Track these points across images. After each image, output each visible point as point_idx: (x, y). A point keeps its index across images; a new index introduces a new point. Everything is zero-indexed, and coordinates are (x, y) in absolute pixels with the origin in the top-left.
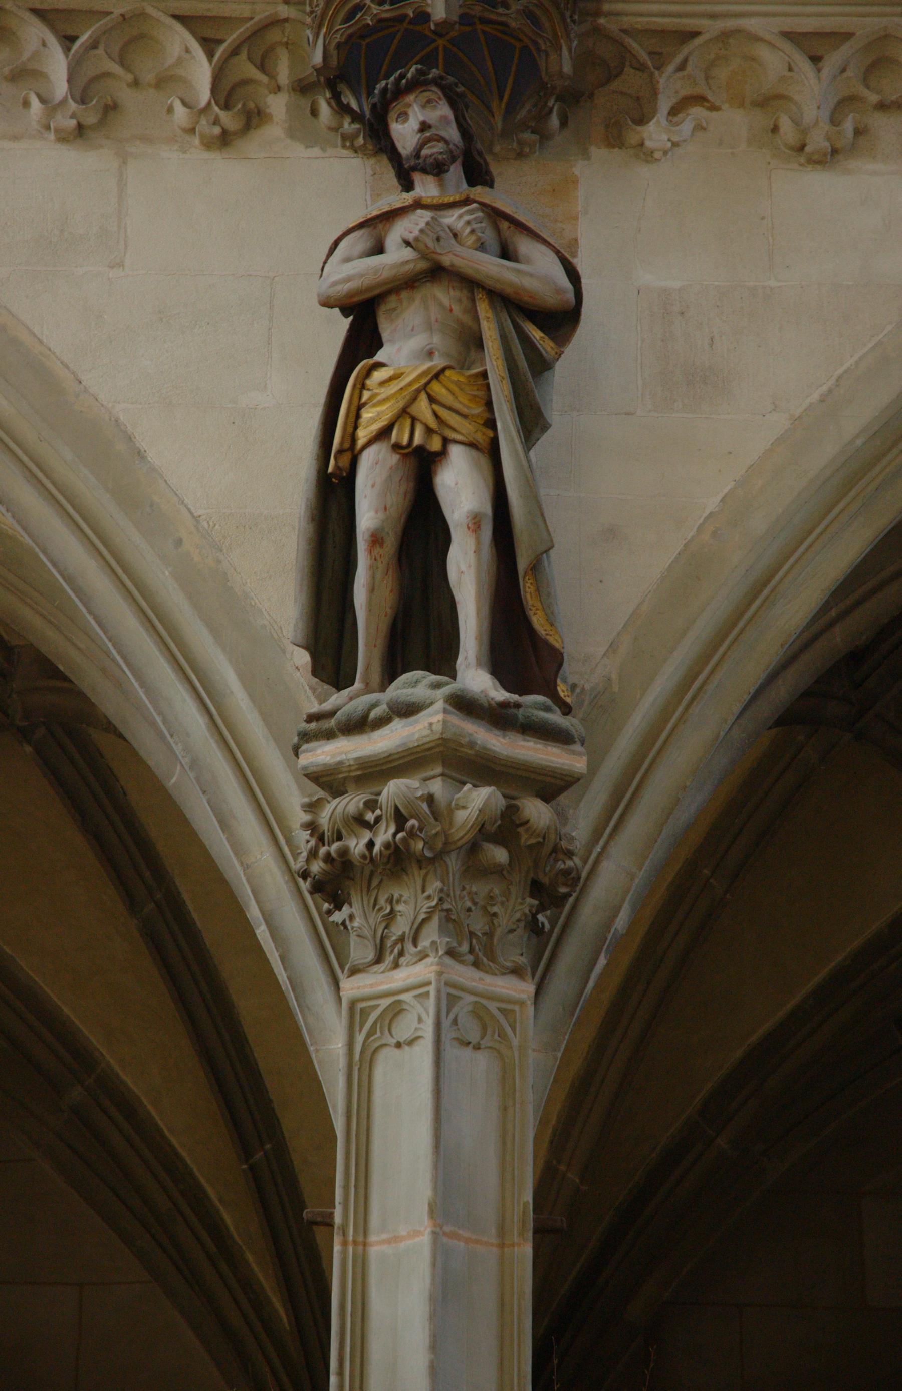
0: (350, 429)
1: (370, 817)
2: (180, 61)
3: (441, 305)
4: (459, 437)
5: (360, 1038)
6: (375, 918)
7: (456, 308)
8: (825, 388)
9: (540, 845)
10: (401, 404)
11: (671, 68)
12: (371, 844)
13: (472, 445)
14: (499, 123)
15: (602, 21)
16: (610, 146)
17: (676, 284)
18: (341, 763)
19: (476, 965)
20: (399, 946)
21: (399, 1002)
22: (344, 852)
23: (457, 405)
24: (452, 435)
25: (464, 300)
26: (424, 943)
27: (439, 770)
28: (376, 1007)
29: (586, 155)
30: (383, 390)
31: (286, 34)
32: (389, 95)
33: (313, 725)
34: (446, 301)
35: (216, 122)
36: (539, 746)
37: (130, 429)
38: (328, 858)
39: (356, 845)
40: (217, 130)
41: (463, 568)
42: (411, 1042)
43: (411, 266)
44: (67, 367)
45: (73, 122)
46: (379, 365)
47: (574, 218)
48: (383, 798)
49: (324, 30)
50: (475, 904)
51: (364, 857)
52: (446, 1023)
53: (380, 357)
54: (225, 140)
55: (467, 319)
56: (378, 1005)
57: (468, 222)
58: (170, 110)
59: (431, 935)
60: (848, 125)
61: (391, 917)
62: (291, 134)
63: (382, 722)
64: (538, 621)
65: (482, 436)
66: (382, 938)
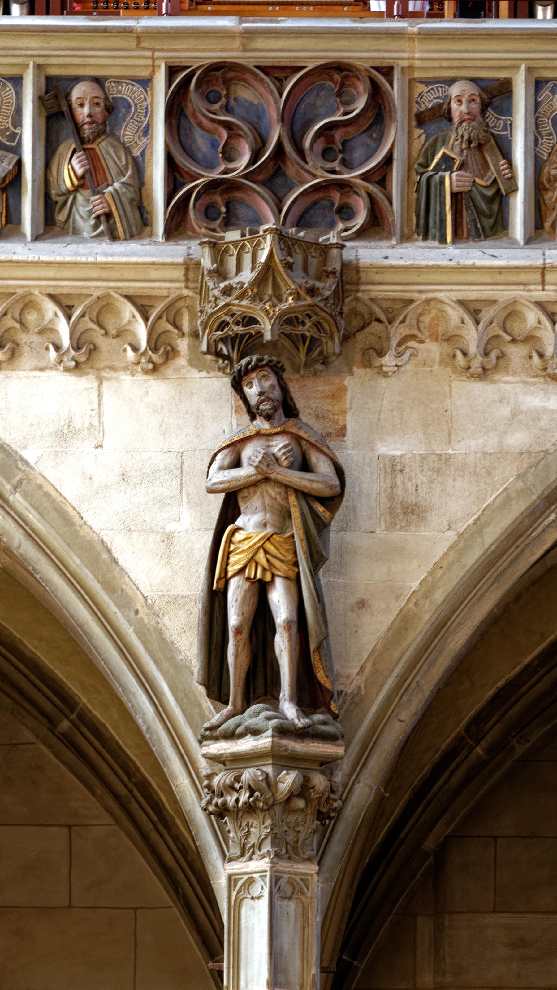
0: (224, 566)
1: (237, 786)
2: (129, 323)
3: (271, 496)
4: (280, 573)
5: (234, 894)
6: (240, 834)
7: (278, 498)
8: (476, 516)
9: (321, 798)
10: (250, 556)
11: (397, 324)
12: (237, 800)
13: (286, 578)
15: (359, 294)
16: (365, 366)
17: (399, 453)
18: (222, 754)
19: (289, 858)
20: (252, 849)
21: (252, 877)
22: (225, 804)
23: (279, 556)
24: (277, 572)
25: (282, 492)
26: (264, 851)
27: (270, 762)
28: (242, 878)
29: (351, 373)
30: (241, 546)
31: (186, 327)
32: (242, 373)
33: (208, 733)
34: (273, 494)
35: (150, 361)
36: (321, 745)
37: (109, 546)
38: (216, 805)
39: (230, 800)
40: (151, 366)
41: (283, 648)
42: (259, 898)
43: (254, 478)
44: (75, 509)
45: (73, 363)
46: (238, 529)
48: (243, 777)
49: (207, 331)
50: (289, 827)
51: (234, 807)
52: (275, 891)
53: (239, 522)
54: (155, 369)
55: (284, 503)
56: (242, 878)
57: (284, 454)
58: (125, 350)
59: (267, 847)
60: (493, 355)
61: (248, 833)
62: (191, 363)
63: (242, 736)
64: (320, 675)
65: (292, 574)
66: (244, 844)
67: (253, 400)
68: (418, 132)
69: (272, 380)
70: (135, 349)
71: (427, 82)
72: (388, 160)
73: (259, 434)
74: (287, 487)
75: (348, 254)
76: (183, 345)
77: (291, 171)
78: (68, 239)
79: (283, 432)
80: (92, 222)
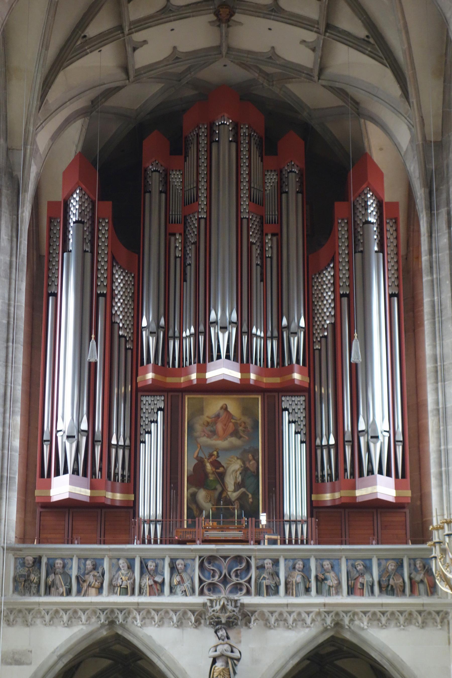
14: (231, 625)
47: (241, 637)
53: (217, 664)
54: (196, 627)
62: (204, 626)
67: (220, 636)
68: (258, 571)
69: (224, 631)
70: (191, 622)
71: (259, 559)
72: (251, 578)
73: (221, 644)
74: (228, 657)
75: (242, 601)
76: (202, 621)
77: (228, 580)
78: (175, 596)
79: (227, 643)
80: (181, 592)
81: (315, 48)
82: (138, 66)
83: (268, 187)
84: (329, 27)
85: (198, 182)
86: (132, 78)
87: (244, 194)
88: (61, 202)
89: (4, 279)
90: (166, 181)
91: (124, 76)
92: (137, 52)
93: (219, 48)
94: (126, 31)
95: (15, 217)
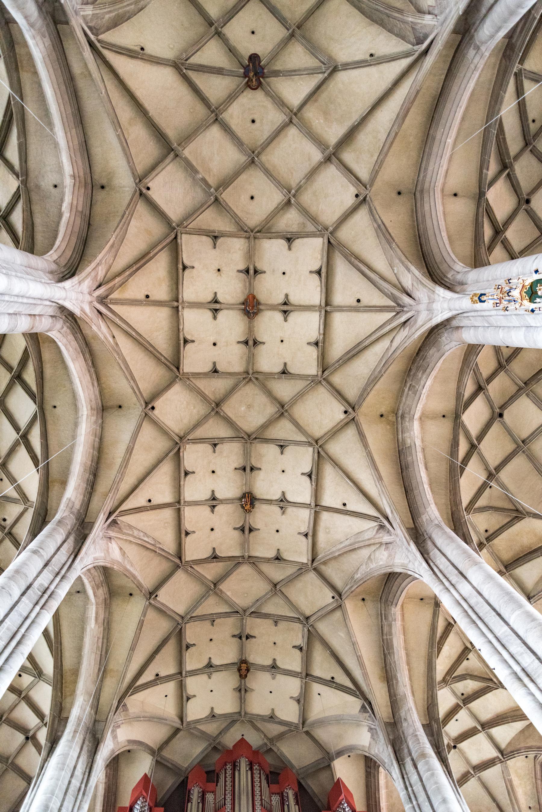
81: (307, 534)
82: (189, 719)
83: (274, 803)
84: (307, 675)
85: (225, 795)
86: (184, 725)
87: (258, 803)
88: (127, 807)
89: (71, 797)
90: (203, 799)
91: (179, 722)
92: (190, 701)
93: (240, 713)
94: (184, 673)
95: (91, 760)
